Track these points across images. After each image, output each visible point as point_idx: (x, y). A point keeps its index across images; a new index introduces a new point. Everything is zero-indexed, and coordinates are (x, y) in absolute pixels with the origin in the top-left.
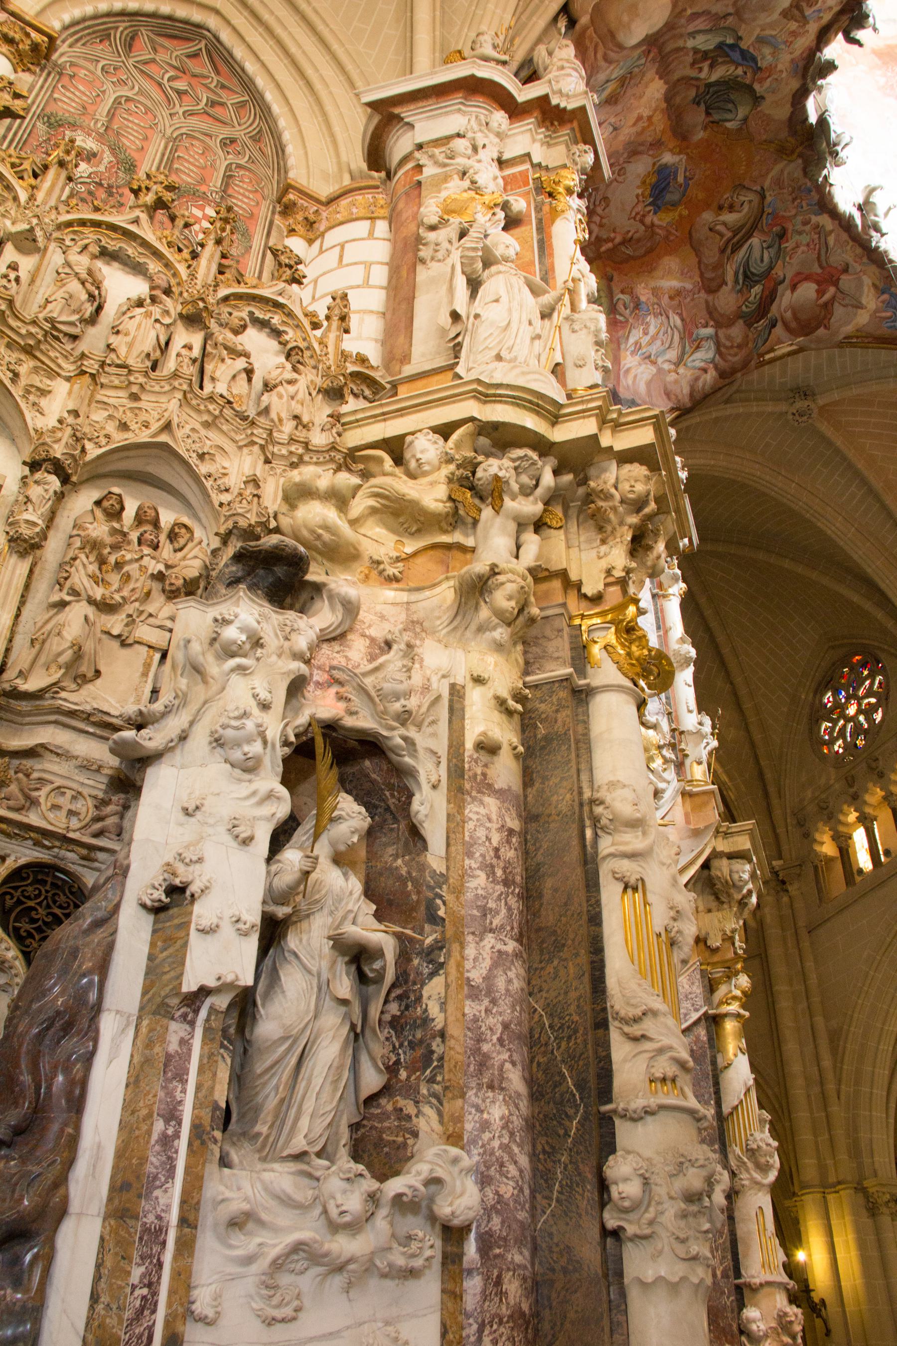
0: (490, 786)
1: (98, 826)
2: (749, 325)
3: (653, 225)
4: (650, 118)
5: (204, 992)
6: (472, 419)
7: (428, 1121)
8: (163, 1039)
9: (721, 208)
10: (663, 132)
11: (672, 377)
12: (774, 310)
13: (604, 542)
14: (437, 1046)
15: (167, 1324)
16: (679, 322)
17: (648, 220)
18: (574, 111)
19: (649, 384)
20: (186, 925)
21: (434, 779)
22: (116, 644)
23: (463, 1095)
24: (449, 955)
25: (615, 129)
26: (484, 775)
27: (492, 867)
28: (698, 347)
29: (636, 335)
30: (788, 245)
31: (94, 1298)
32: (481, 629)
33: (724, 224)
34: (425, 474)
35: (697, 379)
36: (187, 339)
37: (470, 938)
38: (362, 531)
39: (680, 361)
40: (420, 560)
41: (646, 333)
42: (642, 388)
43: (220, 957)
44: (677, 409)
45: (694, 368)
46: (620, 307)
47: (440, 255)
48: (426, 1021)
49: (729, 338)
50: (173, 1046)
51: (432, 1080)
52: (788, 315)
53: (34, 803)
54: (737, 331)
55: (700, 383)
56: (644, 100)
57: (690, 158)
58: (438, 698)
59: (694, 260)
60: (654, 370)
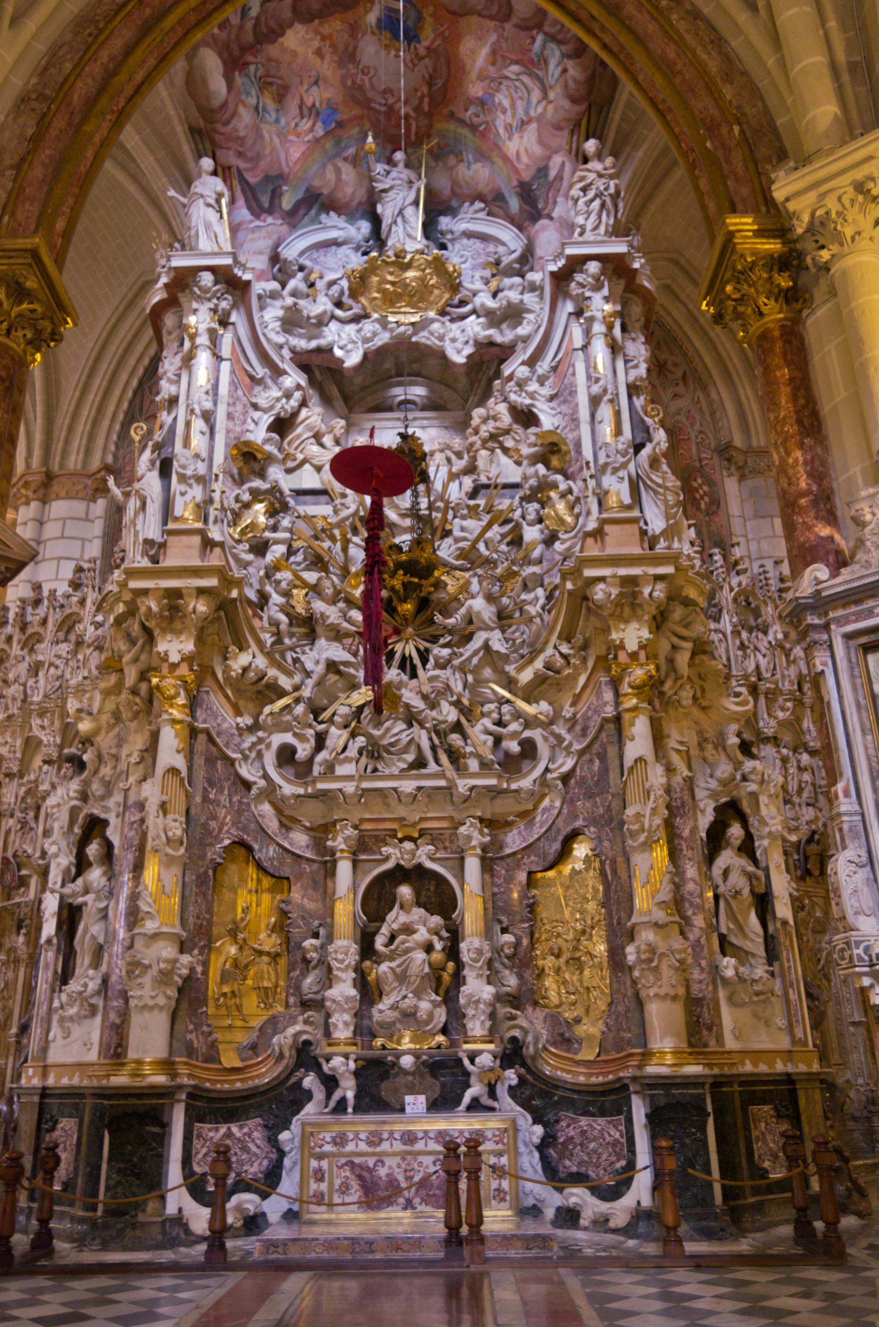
3: (428, 48)
4: (323, 39)
10: (343, 22)
11: (550, 108)
16: (515, 68)
17: (422, 52)
19: (540, 142)
25: (316, 83)
28: (546, 62)
29: (501, 122)
35: (566, 85)
39: (544, 91)
41: (504, 112)
42: (537, 150)
44: (577, 125)
45: (557, 81)
46: (476, 120)
55: (571, 85)
56: (300, 50)
59: (475, 19)
60: (534, 126)
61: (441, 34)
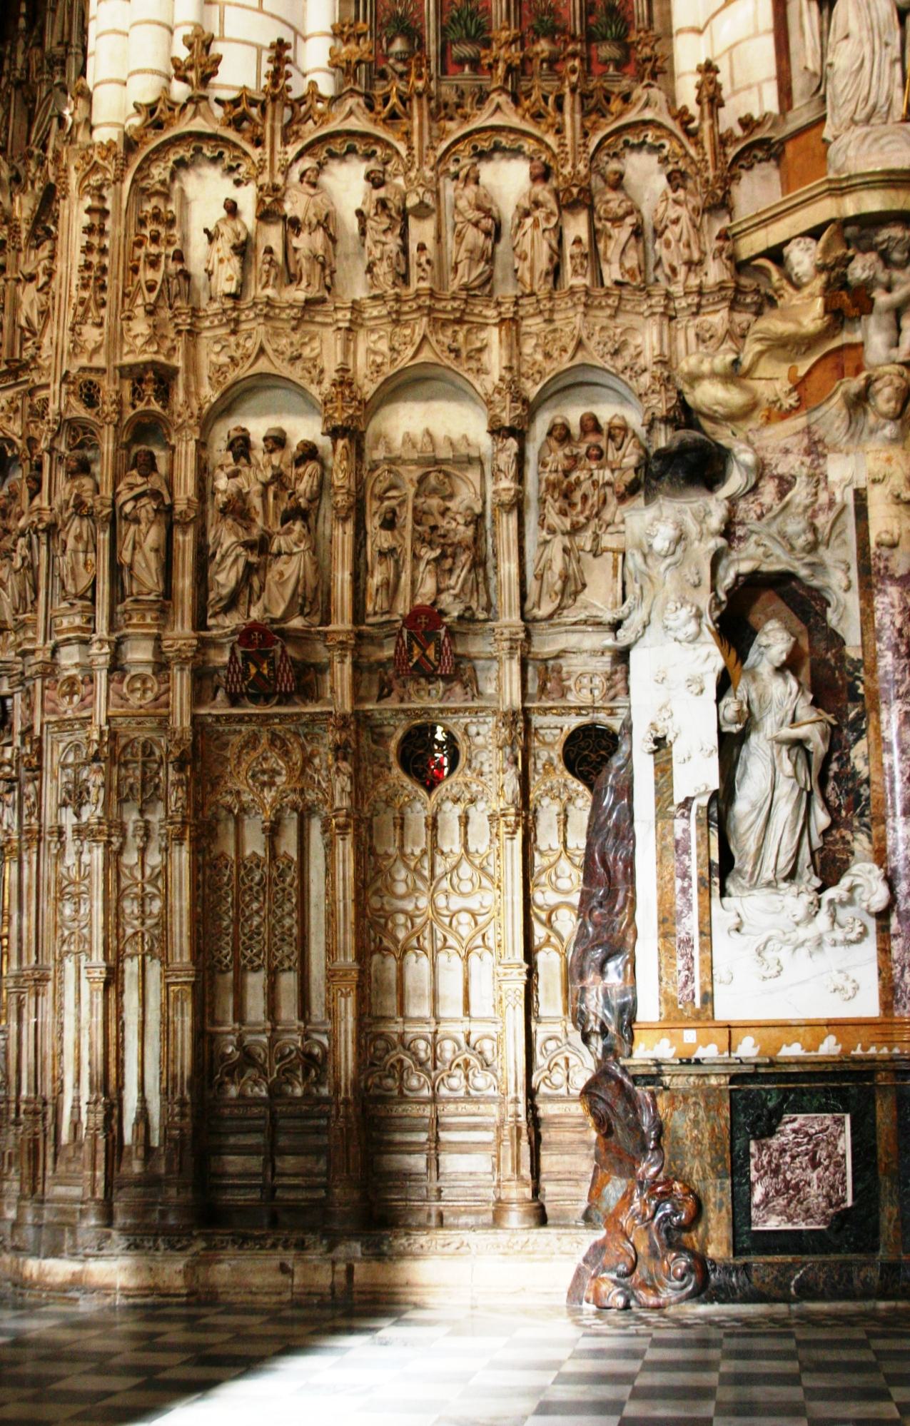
0: (891, 577)
1: (612, 693)
5: (687, 803)
6: (832, 221)
7: (861, 844)
8: (672, 832)
14: (864, 791)
15: (702, 987)
20: (670, 761)
21: (844, 584)
22: (590, 556)
23: (884, 822)
24: (868, 723)
26: (886, 568)
27: (897, 646)
31: (660, 980)
32: (872, 432)
34: (806, 285)
36: (577, 227)
37: (883, 706)
38: (757, 375)
40: (817, 374)
43: (697, 774)
48: (854, 774)
50: (679, 835)
51: (862, 815)
53: (569, 689)
58: (844, 507)
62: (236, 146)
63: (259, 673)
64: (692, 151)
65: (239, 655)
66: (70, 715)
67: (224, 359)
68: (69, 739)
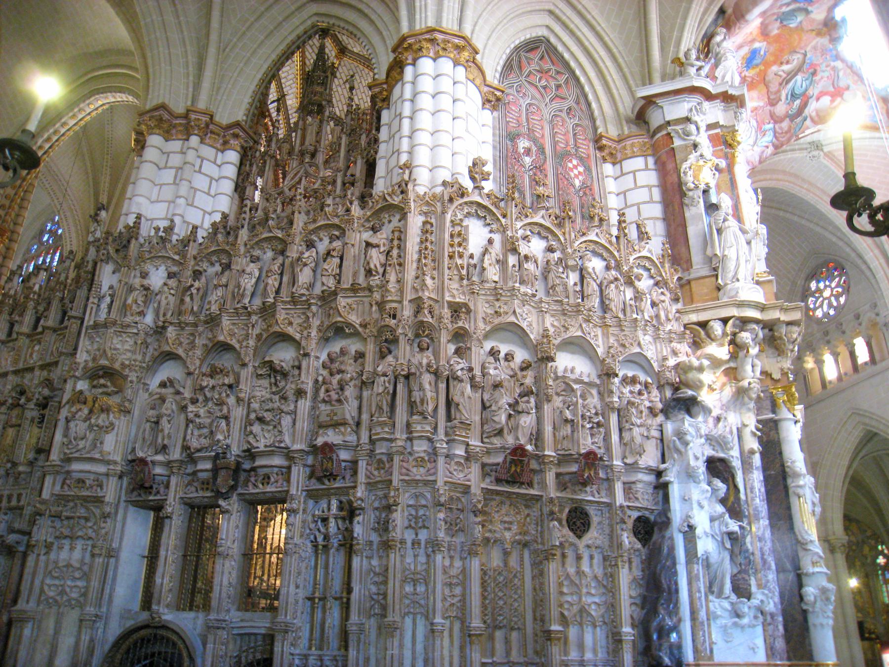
2: (792, 120)
9: (782, 63)
12: (806, 112)
13: (779, 355)
14: (751, 557)
18: (738, 96)
30: (817, 78)
33: (783, 71)
47: (695, 204)
48: (747, 551)
49: (781, 128)
52: (814, 114)
53: (637, 499)
54: (785, 125)
57: (768, 43)
59: (765, 90)
61: (753, 79)
62: (494, 214)
63: (516, 471)
64: (664, 274)
65: (508, 460)
66: (418, 477)
67: (489, 311)
68: (414, 491)
